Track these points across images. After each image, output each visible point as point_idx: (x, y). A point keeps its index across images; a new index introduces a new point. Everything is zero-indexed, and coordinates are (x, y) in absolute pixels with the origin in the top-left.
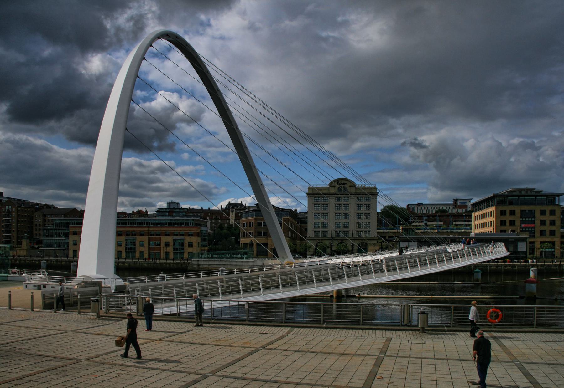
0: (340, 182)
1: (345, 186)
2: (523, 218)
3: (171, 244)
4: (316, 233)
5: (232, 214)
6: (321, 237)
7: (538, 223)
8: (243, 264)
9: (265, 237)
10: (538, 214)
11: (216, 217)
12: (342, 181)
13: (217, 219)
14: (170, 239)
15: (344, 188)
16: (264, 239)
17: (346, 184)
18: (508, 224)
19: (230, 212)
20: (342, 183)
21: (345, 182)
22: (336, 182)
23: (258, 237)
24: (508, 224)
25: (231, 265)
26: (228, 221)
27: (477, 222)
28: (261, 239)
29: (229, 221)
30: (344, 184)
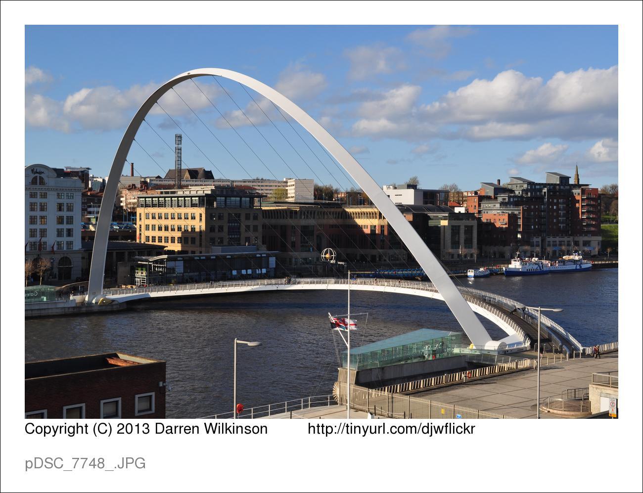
0: (35, 170)
1: (42, 175)
2: (229, 223)
7: (243, 228)
8: (50, 307)
10: (243, 218)
12: (37, 168)
15: (41, 178)
17: (43, 173)
18: (217, 230)
20: (38, 171)
21: (42, 170)
22: (30, 170)
24: (217, 230)
25: (32, 310)
27: (151, 222)
30: (40, 173)
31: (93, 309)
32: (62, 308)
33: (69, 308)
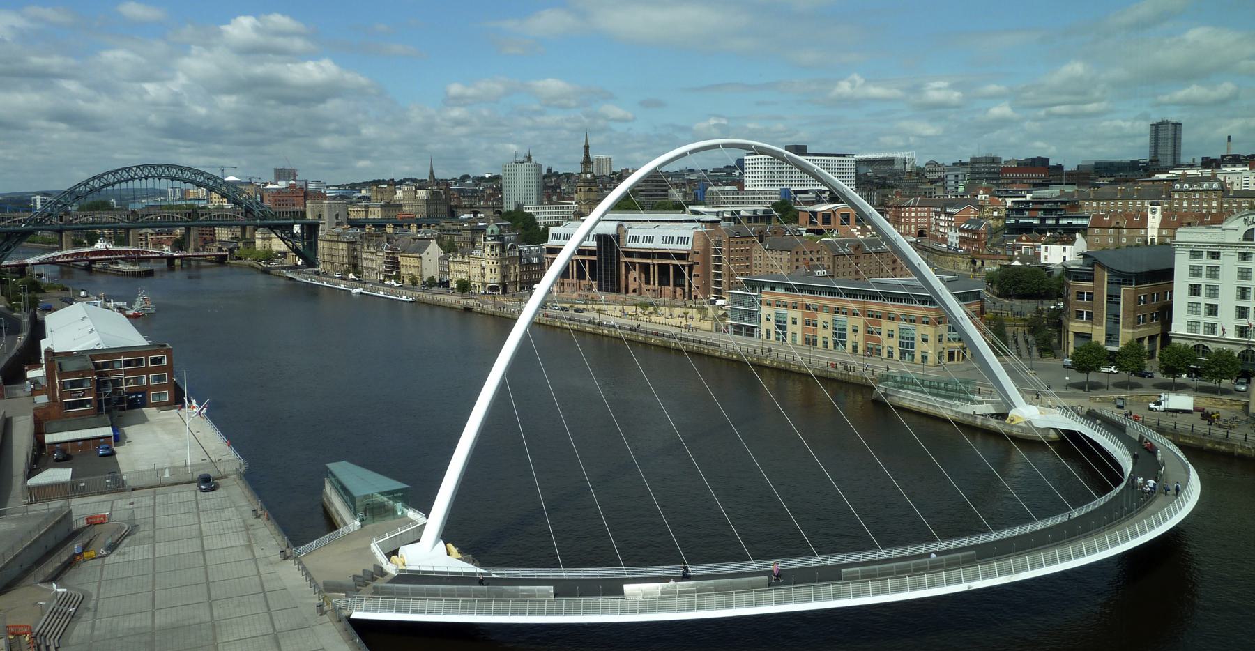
3: (896, 334)
4: (1193, 325)
5: (1153, 217)
6: (1202, 334)
9: (1089, 323)
11: (1118, 223)
12: (1252, 217)
13: (1119, 228)
14: (893, 326)
16: (1088, 325)
19: (1149, 214)
23: (1076, 322)
25: (928, 404)
26: (1142, 232)
28: (1082, 325)
29: (1147, 232)
31: (989, 423)
32: (957, 412)
33: (964, 414)
